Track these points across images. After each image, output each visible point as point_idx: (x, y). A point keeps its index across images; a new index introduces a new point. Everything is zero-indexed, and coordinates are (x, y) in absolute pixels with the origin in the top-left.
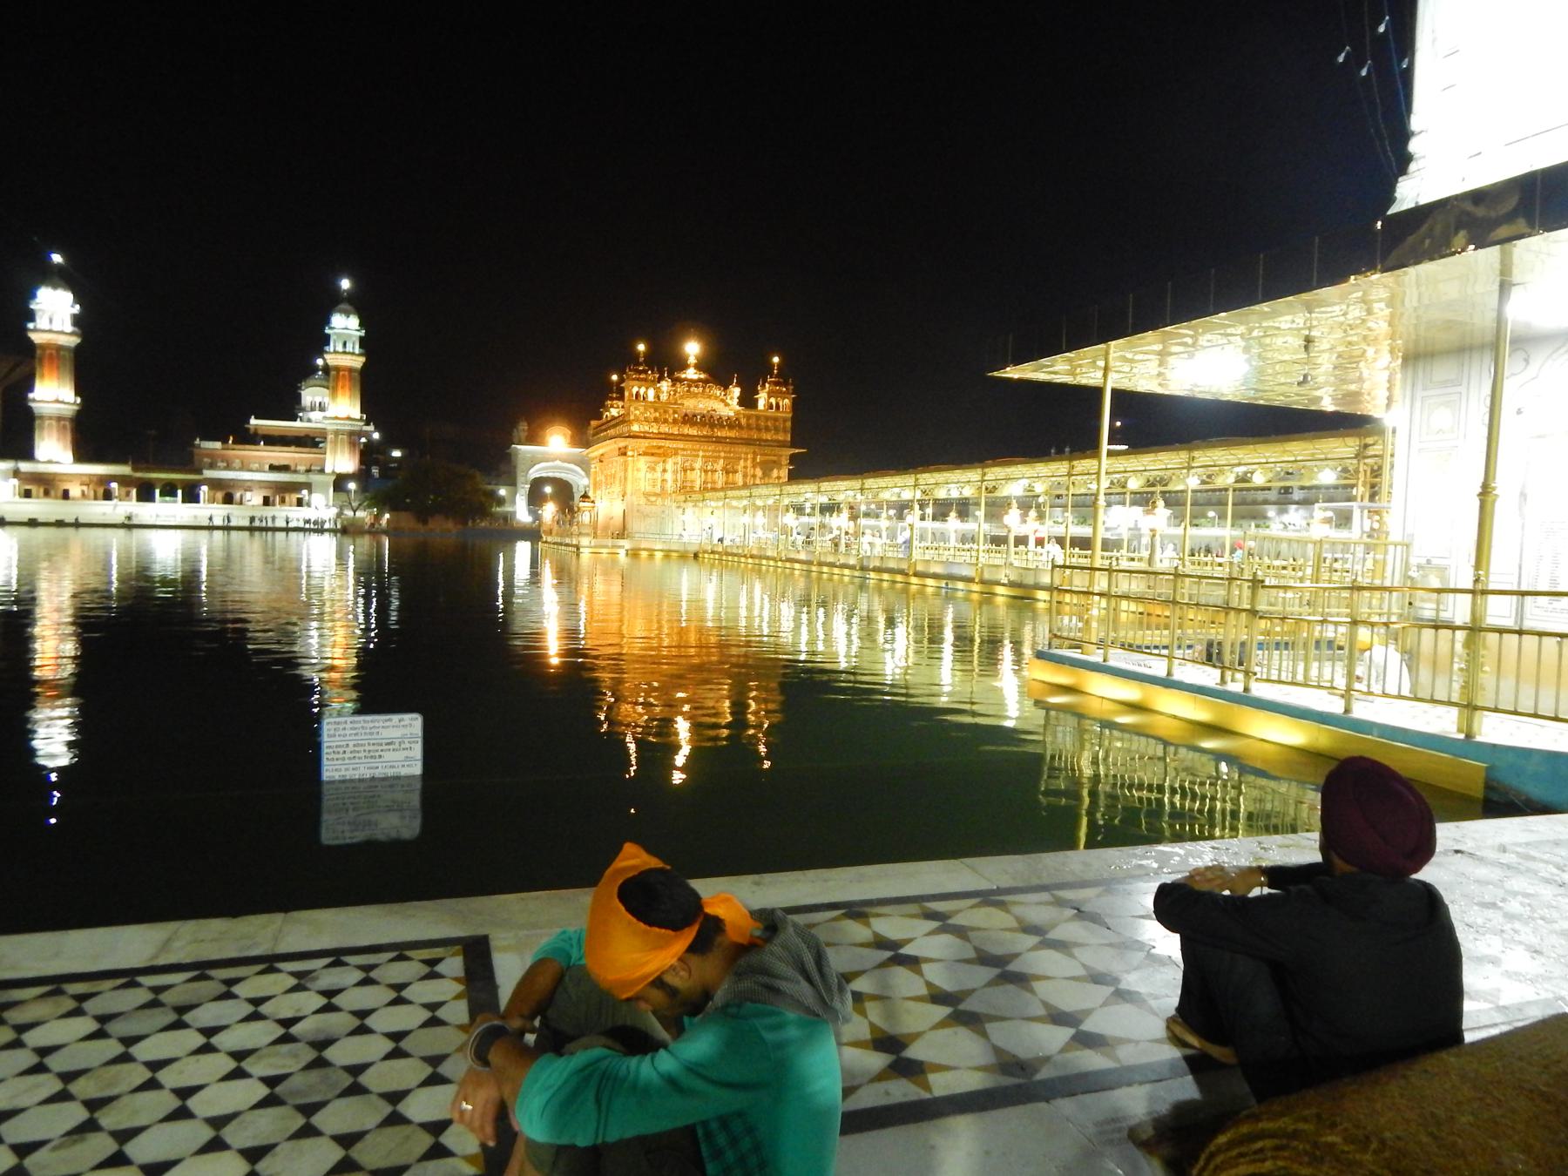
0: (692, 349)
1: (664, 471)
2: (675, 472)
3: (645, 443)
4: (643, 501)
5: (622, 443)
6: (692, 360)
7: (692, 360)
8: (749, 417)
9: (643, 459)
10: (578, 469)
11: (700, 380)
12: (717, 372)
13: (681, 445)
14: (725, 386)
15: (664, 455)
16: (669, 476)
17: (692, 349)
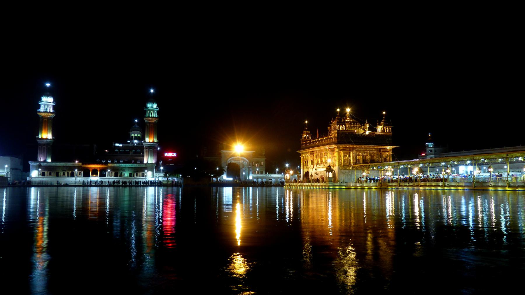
0: (348, 110)
1: (349, 156)
2: (353, 157)
3: (342, 146)
4: (343, 168)
5: (332, 147)
6: (348, 115)
7: (348, 115)
8: (376, 135)
9: (342, 152)
10: (246, 159)
11: (353, 122)
12: (359, 118)
13: (355, 146)
14: (363, 124)
15: (350, 150)
16: (351, 158)
17: (348, 110)
